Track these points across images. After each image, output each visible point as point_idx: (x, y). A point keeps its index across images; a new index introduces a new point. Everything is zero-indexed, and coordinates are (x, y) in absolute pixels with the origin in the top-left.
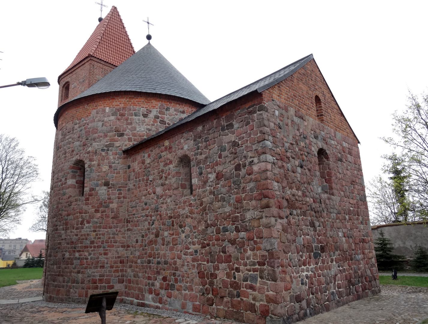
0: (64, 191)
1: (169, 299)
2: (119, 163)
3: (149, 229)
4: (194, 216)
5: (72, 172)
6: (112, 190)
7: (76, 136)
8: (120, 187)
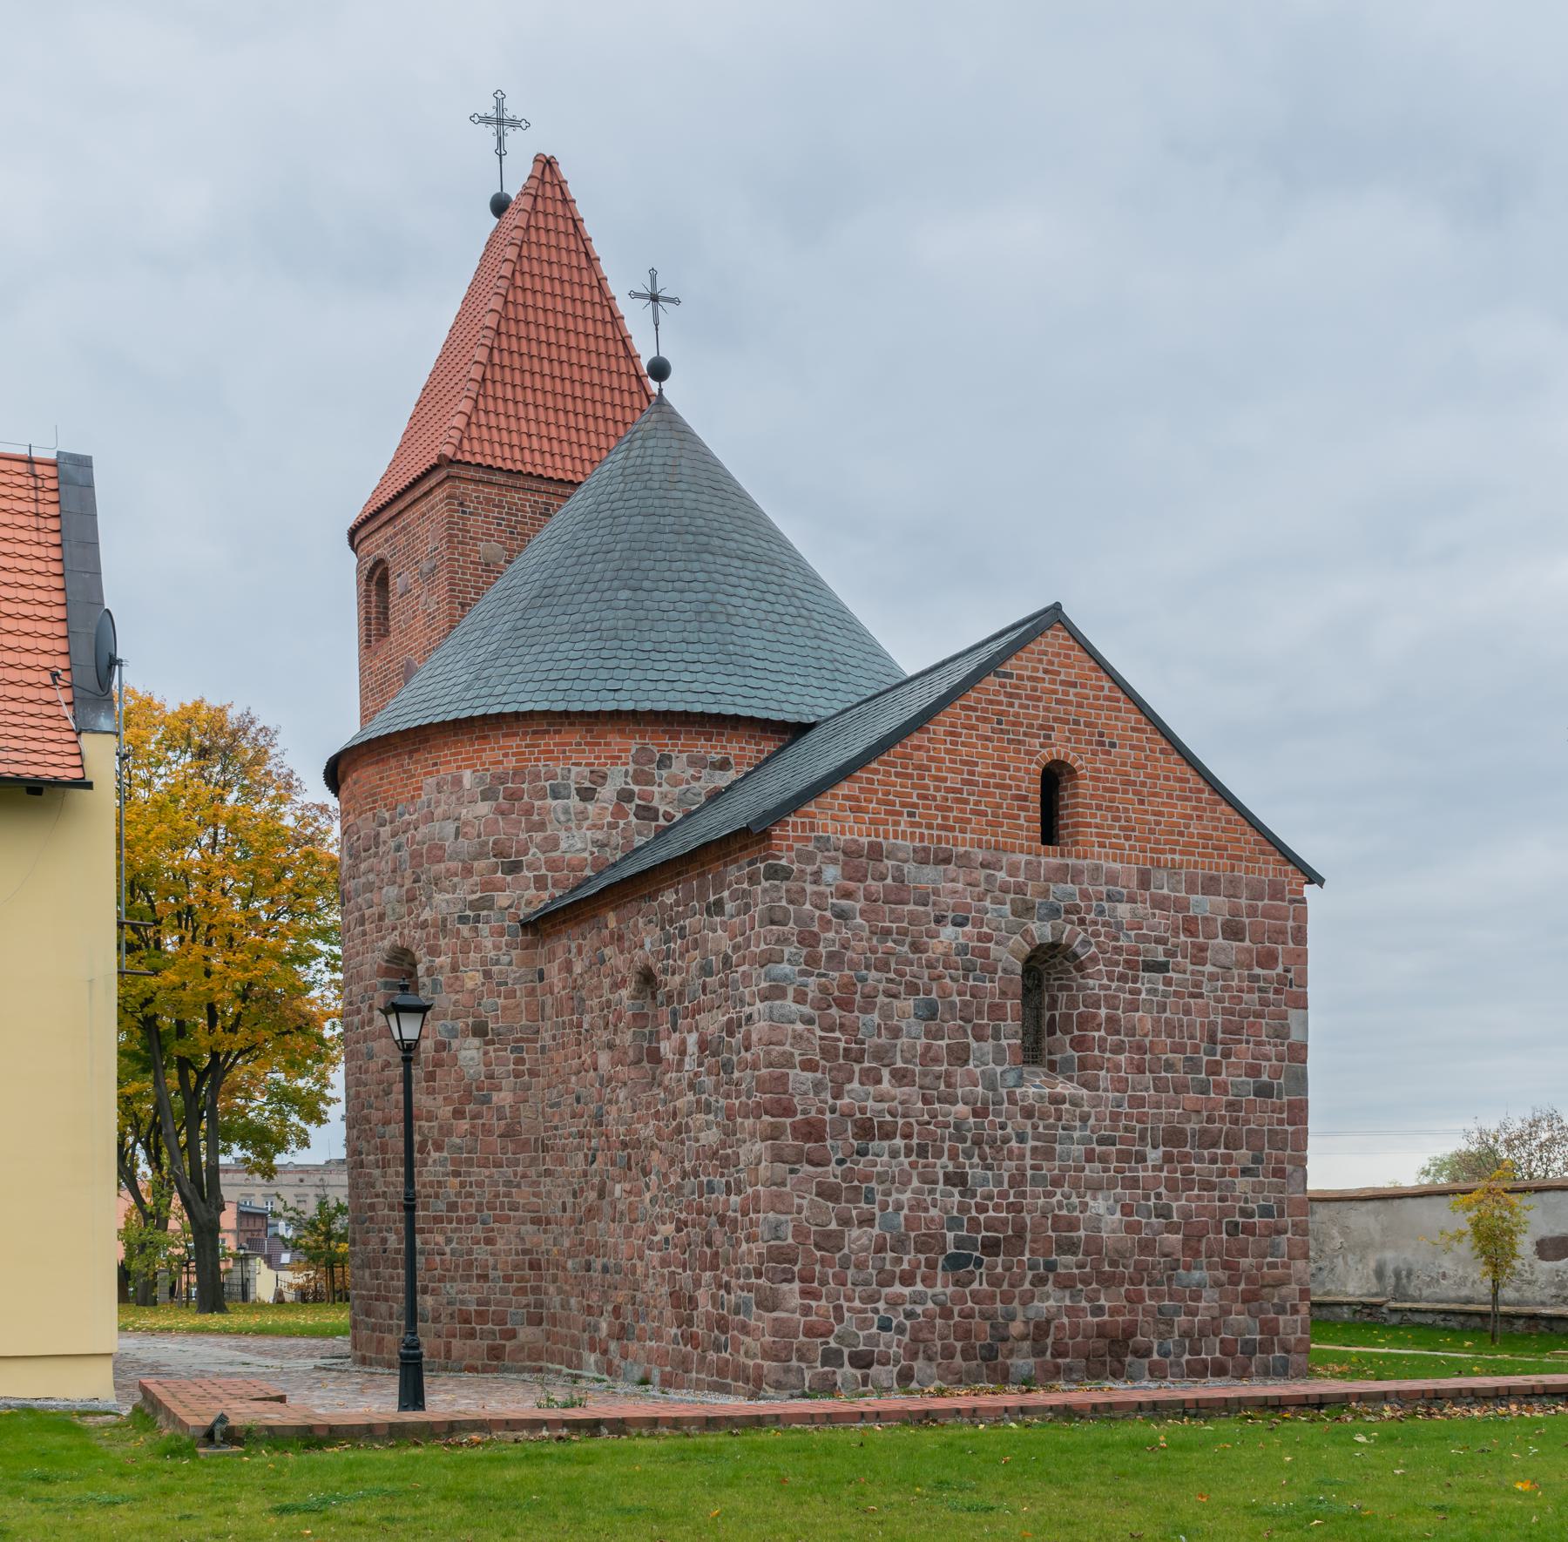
0: (370, 1044)
1: (623, 1364)
2: (511, 962)
3: (585, 1174)
4: (663, 1144)
5: (386, 985)
6: (495, 1051)
7: (386, 866)
8: (517, 1041)
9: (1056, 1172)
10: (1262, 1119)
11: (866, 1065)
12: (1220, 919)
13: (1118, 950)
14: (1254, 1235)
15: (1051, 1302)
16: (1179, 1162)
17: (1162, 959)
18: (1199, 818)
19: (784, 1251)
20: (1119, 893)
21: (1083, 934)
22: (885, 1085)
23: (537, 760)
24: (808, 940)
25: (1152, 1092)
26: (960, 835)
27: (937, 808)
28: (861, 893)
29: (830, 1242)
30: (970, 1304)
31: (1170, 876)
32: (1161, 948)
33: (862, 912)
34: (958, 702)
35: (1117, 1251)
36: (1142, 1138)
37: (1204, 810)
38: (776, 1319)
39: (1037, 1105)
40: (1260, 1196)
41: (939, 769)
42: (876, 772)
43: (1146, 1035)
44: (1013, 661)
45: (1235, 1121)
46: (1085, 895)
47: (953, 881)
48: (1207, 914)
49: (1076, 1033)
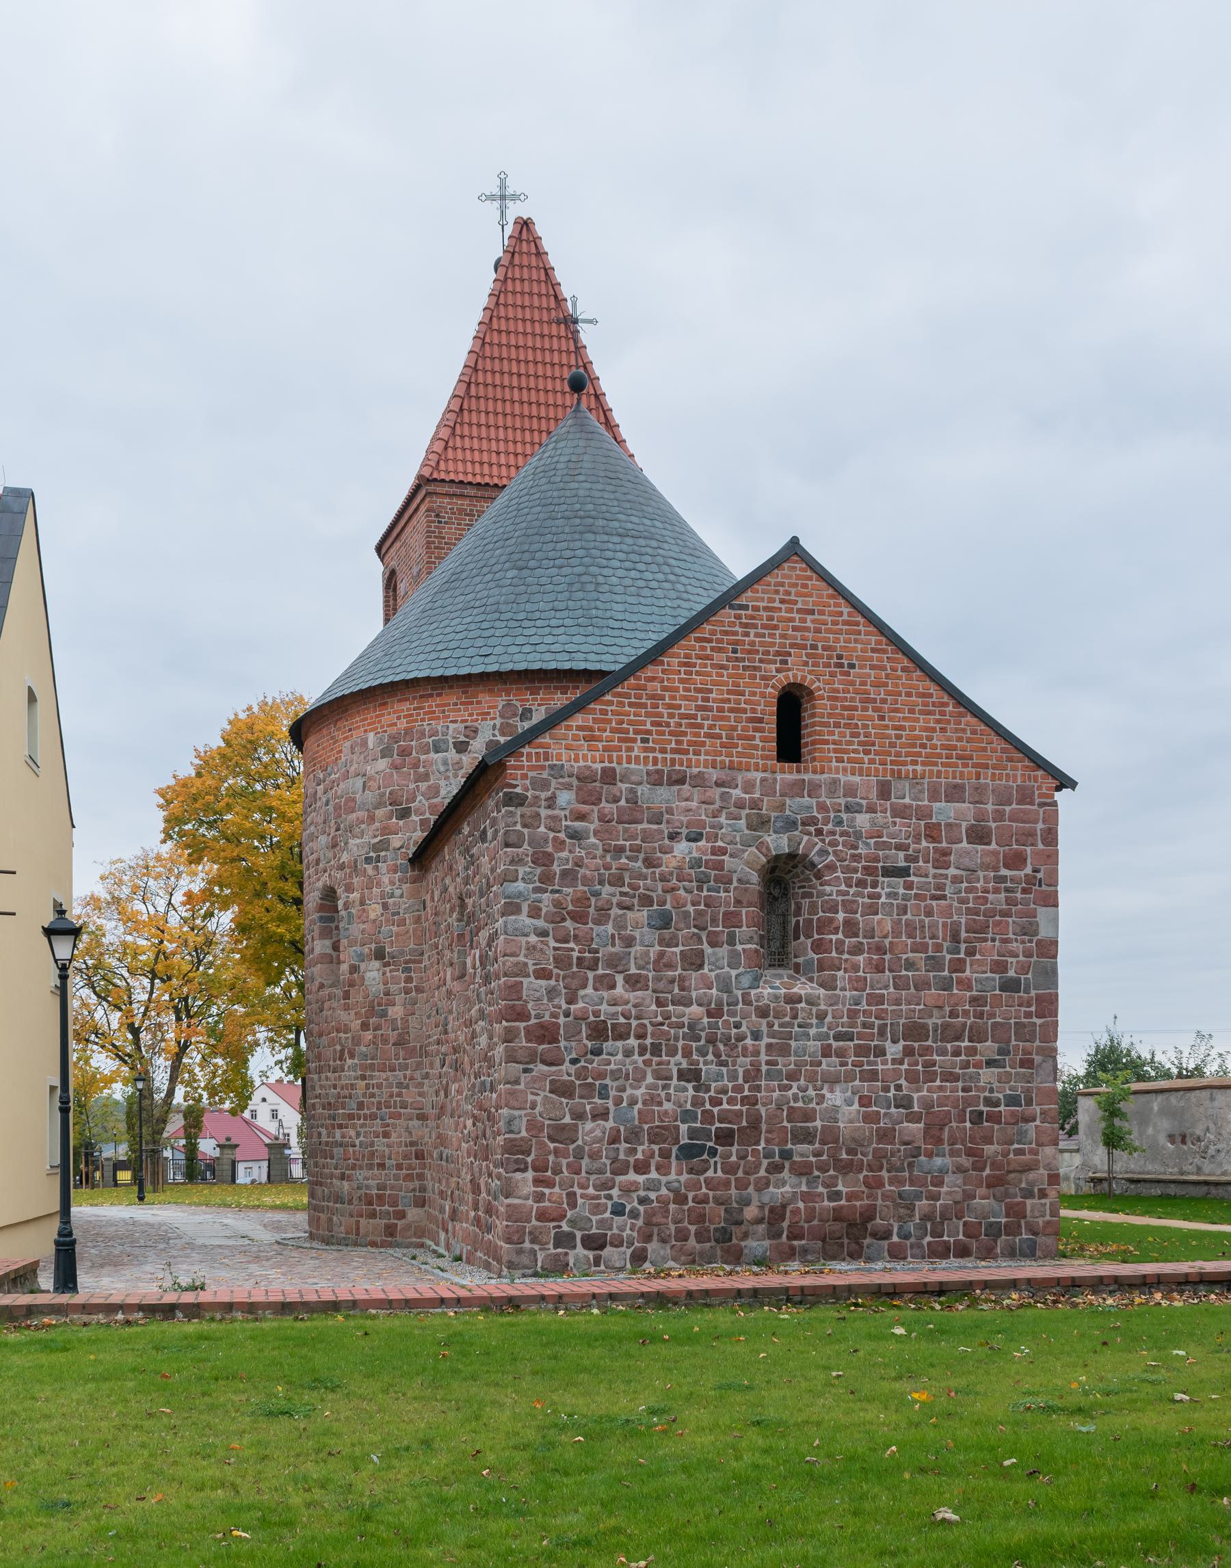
7: (320, 820)
8: (407, 962)
9: (792, 1066)
10: (1009, 1012)
11: (600, 972)
12: (964, 824)
13: (857, 858)
14: (999, 1123)
15: (787, 1188)
16: (920, 1055)
17: (902, 864)
18: (943, 730)
19: (518, 1143)
20: (858, 804)
21: (820, 844)
22: (619, 990)
23: (423, 720)
24: (543, 859)
25: (892, 990)
26: (694, 757)
27: (671, 733)
28: (596, 815)
29: (563, 1134)
30: (704, 1190)
31: (912, 786)
32: (901, 854)
33: (596, 833)
34: (693, 635)
35: (854, 1140)
36: (882, 1033)
37: (948, 722)
38: (509, 1206)
39: (772, 1005)
40: (1007, 1086)
41: (673, 698)
42: (610, 703)
43: (886, 937)
44: (749, 594)
45: (980, 1015)
46: (822, 807)
47: (687, 800)
48: (951, 820)
49: (816, 936)
